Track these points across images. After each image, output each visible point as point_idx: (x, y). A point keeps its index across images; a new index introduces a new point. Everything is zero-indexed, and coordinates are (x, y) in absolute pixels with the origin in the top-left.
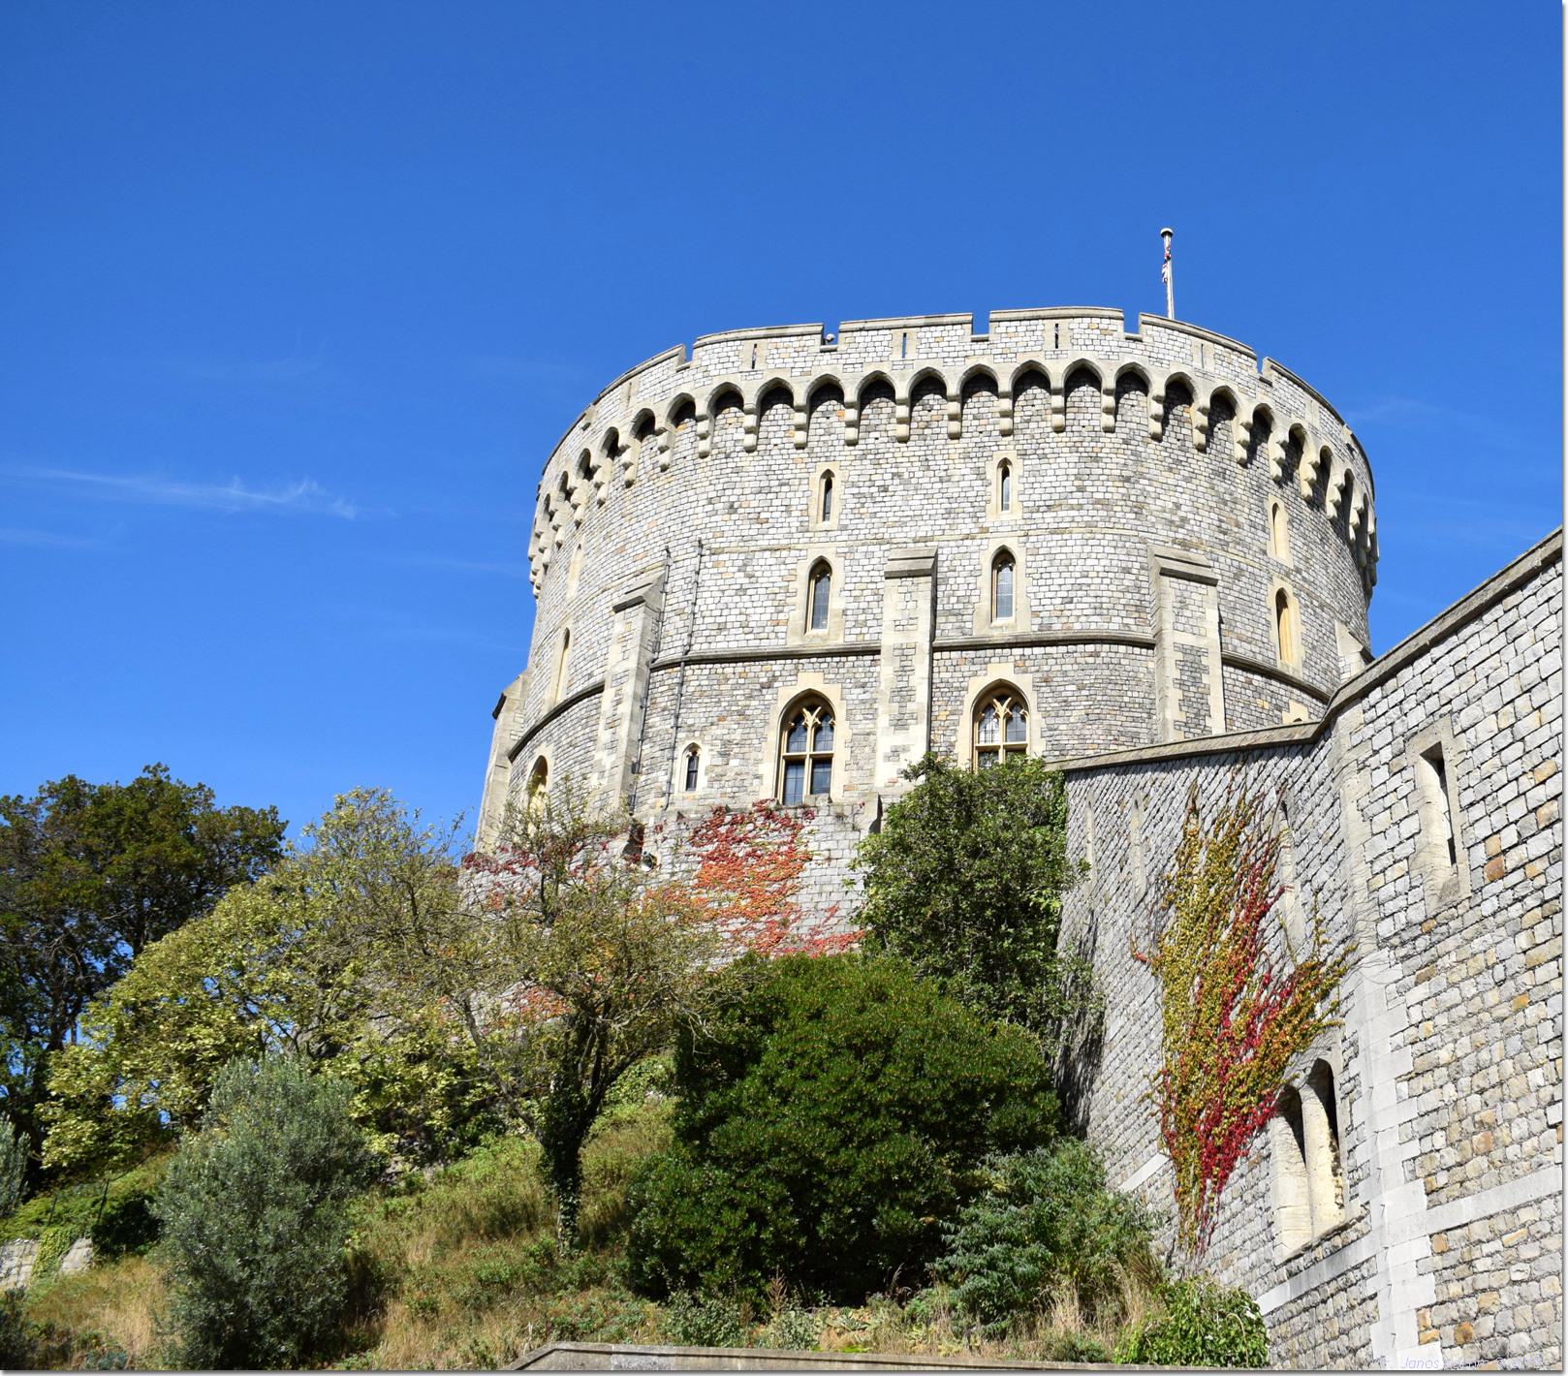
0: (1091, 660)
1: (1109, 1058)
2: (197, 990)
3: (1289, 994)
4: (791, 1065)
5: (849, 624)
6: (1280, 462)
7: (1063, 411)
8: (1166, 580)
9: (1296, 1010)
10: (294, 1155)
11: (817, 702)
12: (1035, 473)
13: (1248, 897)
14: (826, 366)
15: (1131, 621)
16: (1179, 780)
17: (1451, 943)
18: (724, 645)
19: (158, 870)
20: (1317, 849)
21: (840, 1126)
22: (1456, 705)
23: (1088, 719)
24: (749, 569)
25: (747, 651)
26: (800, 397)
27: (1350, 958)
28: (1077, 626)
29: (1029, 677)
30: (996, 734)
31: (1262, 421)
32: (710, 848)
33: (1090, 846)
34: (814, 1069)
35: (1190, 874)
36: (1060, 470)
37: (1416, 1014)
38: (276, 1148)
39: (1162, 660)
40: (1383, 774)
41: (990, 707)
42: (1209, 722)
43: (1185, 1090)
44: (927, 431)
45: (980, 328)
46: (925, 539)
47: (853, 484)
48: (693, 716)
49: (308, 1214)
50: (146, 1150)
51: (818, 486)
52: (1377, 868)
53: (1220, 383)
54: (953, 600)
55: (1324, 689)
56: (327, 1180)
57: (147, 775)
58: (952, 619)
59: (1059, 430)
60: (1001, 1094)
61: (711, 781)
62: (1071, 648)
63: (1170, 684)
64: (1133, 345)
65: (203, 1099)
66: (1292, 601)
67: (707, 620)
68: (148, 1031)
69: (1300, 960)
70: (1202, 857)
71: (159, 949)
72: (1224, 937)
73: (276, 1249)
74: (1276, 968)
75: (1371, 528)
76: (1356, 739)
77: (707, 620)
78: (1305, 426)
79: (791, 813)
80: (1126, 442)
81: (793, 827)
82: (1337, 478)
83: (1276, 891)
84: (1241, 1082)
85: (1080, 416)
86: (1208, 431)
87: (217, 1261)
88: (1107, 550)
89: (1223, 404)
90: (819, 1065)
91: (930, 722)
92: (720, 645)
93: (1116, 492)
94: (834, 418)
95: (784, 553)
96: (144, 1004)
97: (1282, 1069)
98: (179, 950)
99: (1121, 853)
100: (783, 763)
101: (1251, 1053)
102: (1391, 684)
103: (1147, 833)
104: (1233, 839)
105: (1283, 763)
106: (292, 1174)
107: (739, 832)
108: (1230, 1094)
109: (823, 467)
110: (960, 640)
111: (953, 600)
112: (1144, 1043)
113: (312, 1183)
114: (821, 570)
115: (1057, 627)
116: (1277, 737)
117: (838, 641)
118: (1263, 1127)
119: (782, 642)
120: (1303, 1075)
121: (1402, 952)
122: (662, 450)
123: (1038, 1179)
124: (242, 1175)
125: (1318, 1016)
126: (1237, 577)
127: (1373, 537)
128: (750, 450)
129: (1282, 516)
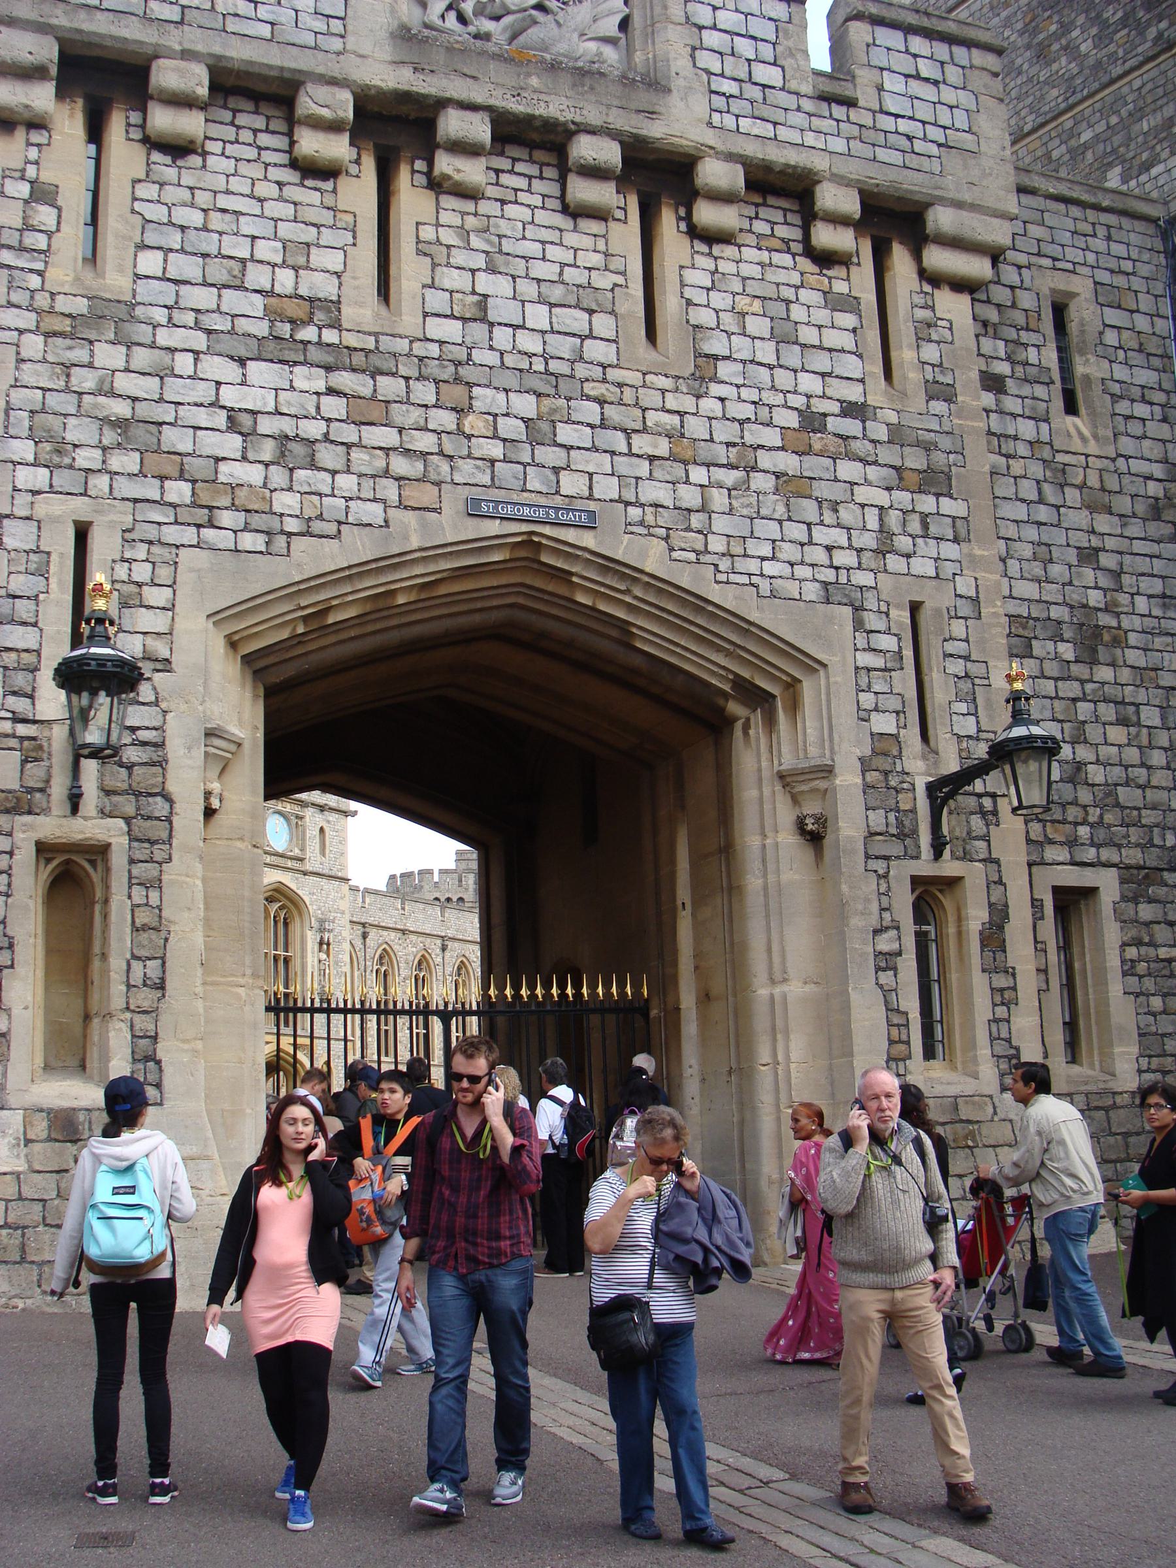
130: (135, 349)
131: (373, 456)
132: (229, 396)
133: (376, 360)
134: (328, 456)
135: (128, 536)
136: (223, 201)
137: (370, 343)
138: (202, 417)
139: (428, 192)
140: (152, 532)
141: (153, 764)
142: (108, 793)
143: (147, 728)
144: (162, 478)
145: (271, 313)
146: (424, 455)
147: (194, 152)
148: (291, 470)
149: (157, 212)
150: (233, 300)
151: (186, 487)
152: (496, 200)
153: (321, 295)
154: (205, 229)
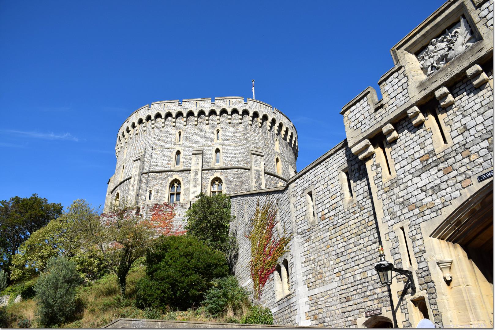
0: (236, 173)
1: (240, 258)
2: (44, 242)
3: (278, 244)
4: (171, 259)
5: (184, 165)
6: (277, 130)
7: (231, 119)
8: (253, 155)
9: (280, 248)
10: (64, 278)
11: (177, 181)
12: (225, 132)
13: (270, 224)
14: (180, 109)
15: (245, 164)
16: (255, 198)
17: (313, 234)
18: (157, 169)
19: (35, 216)
20: (285, 213)
21: (182, 272)
22: (315, 183)
23: (235, 185)
24: (163, 153)
25: (162, 170)
26: (174, 116)
27: (292, 237)
28: (233, 165)
29: (223, 176)
30: (216, 188)
31: (273, 122)
32: (154, 212)
33: (236, 213)
34: (176, 260)
35: (257, 219)
36: (230, 132)
37: (306, 249)
38: (61, 276)
39: (251, 173)
40: (299, 197)
41: (215, 182)
42: (262, 186)
43: (256, 265)
44: (201, 123)
45: (213, 101)
46: (201, 146)
47: (185, 135)
48: (151, 184)
49: (67, 290)
50: (33, 276)
51: (178, 135)
52: (298, 217)
53: (265, 113)
54: (207, 159)
55: (286, 179)
56: (71, 283)
57: (33, 196)
58: (206, 163)
59: (230, 123)
60: (216, 265)
61: (154, 198)
62: (232, 170)
63: (253, 178)
64: (246, 105)
65: (45, 266)
66: (280, 160)
67: (154, 163)
68: (33, 251)
69: (281, 237)
70: (260, 215)
71: (36, 233)
72: (264, 232)
73: (60, 298)
74: (276, 239)
75: (297, 144)
76: (293, 190)
77: (154, 163)
78: (283, 122)
79: (171, 205)
80: (244, 126)
81: (172, 208)
82: (289, 134)
83: (276, 222)
84: (268, 263)
85: (234, 120)
86: (262, 124)
87: (48, 300)
88: (240, 149)
89: (265, 118)
90: (177, 259)
91: (201, 186)
92: (156, 169)
93: (242, 136)
94: (181, 120)
95: (170, 149)
96: (32, 245)
97: (277, 261)
98: (40, 233)
99: (242, 214)
100: (170, 194)
101: (270, 257)
102: (301, 178)
103: (248, 210)
104: (267, 211)
105: (278, 195)
106: (64, 282)
107: (160, 209)
108: (265, 266)
109: (179, 131)
110: (208, 168)
111: (207, 159)
112: (247, 255)
113: (68, 284)
114: (178, 153)
115: (229, 165)
116: (276, 189)
117: (182, 168)
118: (273, 273)
119: (170, 168)
120: (281, 262)
121: (303, 236)
122: (144, 127)
123: (224, 284)
124: (53, 282)
125: (285, 249)
126: (268, 155)
127: (297, 146)
128: (163, 127)
129: (278, 142)
130: (401, 186)
131: (452, 180)
132: (420, 185)
133: (446, 157)
134: (443, 186)
135: (410, 226)
136: (406, 145)
137: (443, 154)
138: (416, 193)
139: (443, 110)
140: (414, 223)
141: (428, 275)
142: (421, 285)
143: (425, 267)
144: (412, 210)
145: (422, 162)
146: (464, 173)
147: (398, 139)
148: (436, 194)
149: (396, 155)
150: (414, 164)
151: (417, 210)
152: (459, 100)
153: (430, 151)
154: (405, 152)
